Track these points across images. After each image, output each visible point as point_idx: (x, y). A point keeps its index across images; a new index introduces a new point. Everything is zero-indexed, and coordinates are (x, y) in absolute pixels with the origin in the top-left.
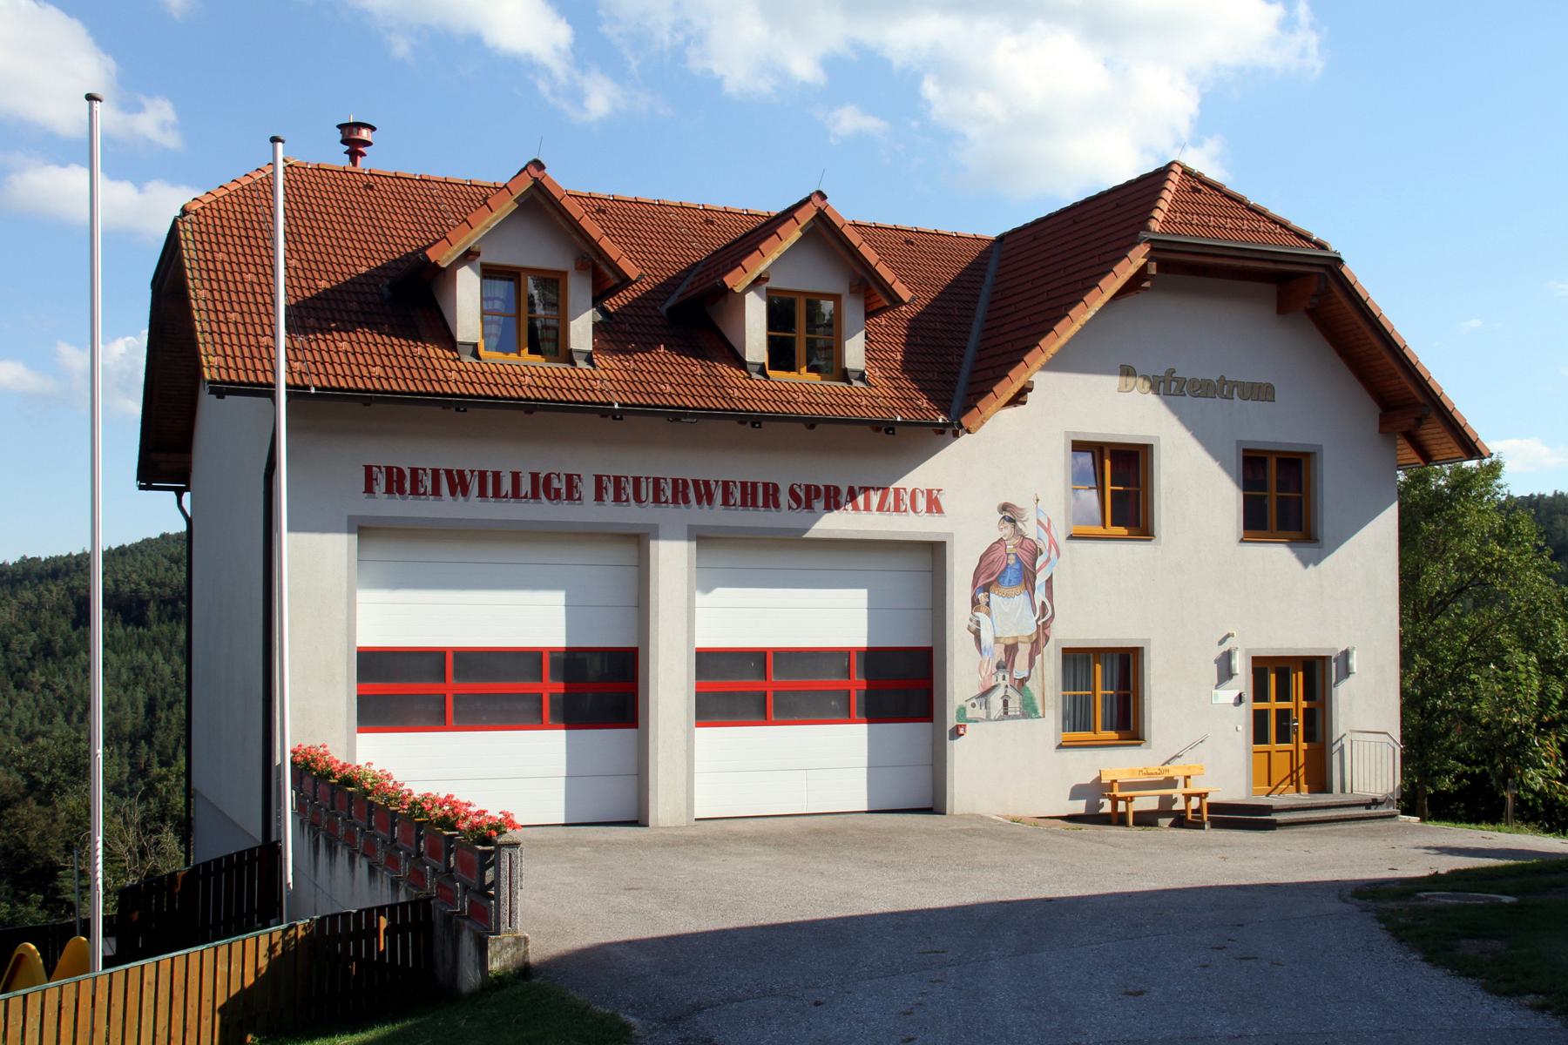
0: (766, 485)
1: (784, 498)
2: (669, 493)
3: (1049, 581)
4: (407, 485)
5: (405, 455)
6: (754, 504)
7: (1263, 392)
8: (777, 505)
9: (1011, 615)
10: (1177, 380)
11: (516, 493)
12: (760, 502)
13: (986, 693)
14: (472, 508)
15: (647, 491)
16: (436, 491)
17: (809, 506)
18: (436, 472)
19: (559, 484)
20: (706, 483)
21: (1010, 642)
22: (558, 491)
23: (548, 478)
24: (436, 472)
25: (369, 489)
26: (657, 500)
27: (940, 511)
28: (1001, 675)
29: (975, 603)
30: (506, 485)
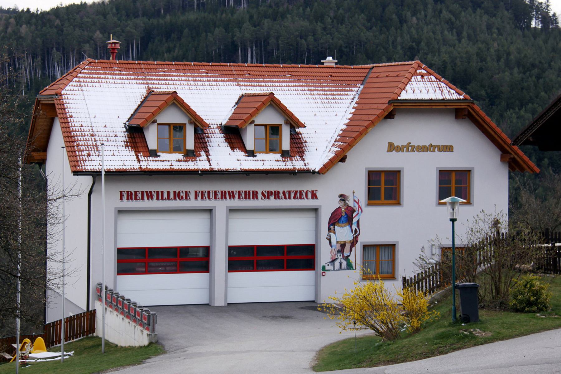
0: (253, 192)
1: (260, 195)
2: (220, 196)
3: (358, 222)
4: (133, 197)
5: (133, 187)
6: (249, 198)
7: (449, 149)
8: (257, 198)
9: (343, 233)
10: (411, 146)
11: (169, 198)
12: (251, 197)
13: (333, 261)
14: (155, 204)
15: (212, 195)
16: (143, 199)
17: (268, 198)
18: (142, 192)
19: (183, 194)
20: (233, 192)
21: (342, 243)
22: (182, 197)
23: (179, 192)
24: (142, 192)
25: (121, 199)
26: (215, 198)
27: (316, 198)
28: (339, 255)
29: (329, 230)
30: (165, 196)
